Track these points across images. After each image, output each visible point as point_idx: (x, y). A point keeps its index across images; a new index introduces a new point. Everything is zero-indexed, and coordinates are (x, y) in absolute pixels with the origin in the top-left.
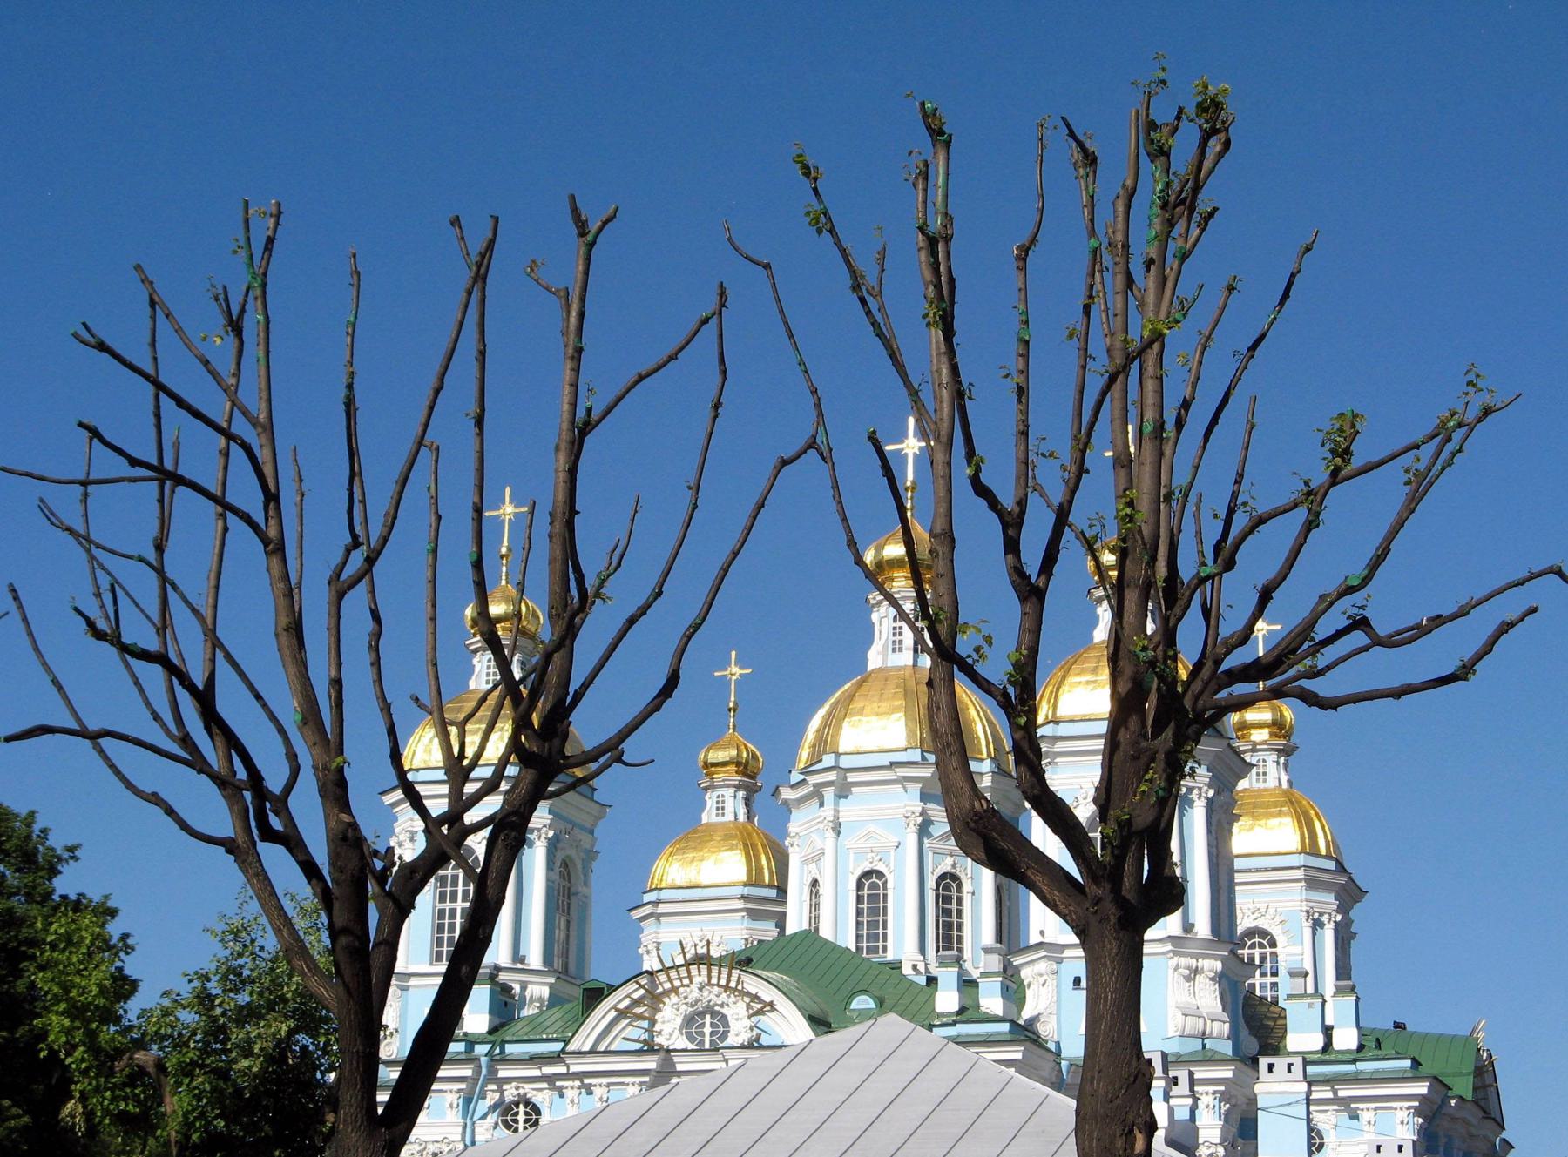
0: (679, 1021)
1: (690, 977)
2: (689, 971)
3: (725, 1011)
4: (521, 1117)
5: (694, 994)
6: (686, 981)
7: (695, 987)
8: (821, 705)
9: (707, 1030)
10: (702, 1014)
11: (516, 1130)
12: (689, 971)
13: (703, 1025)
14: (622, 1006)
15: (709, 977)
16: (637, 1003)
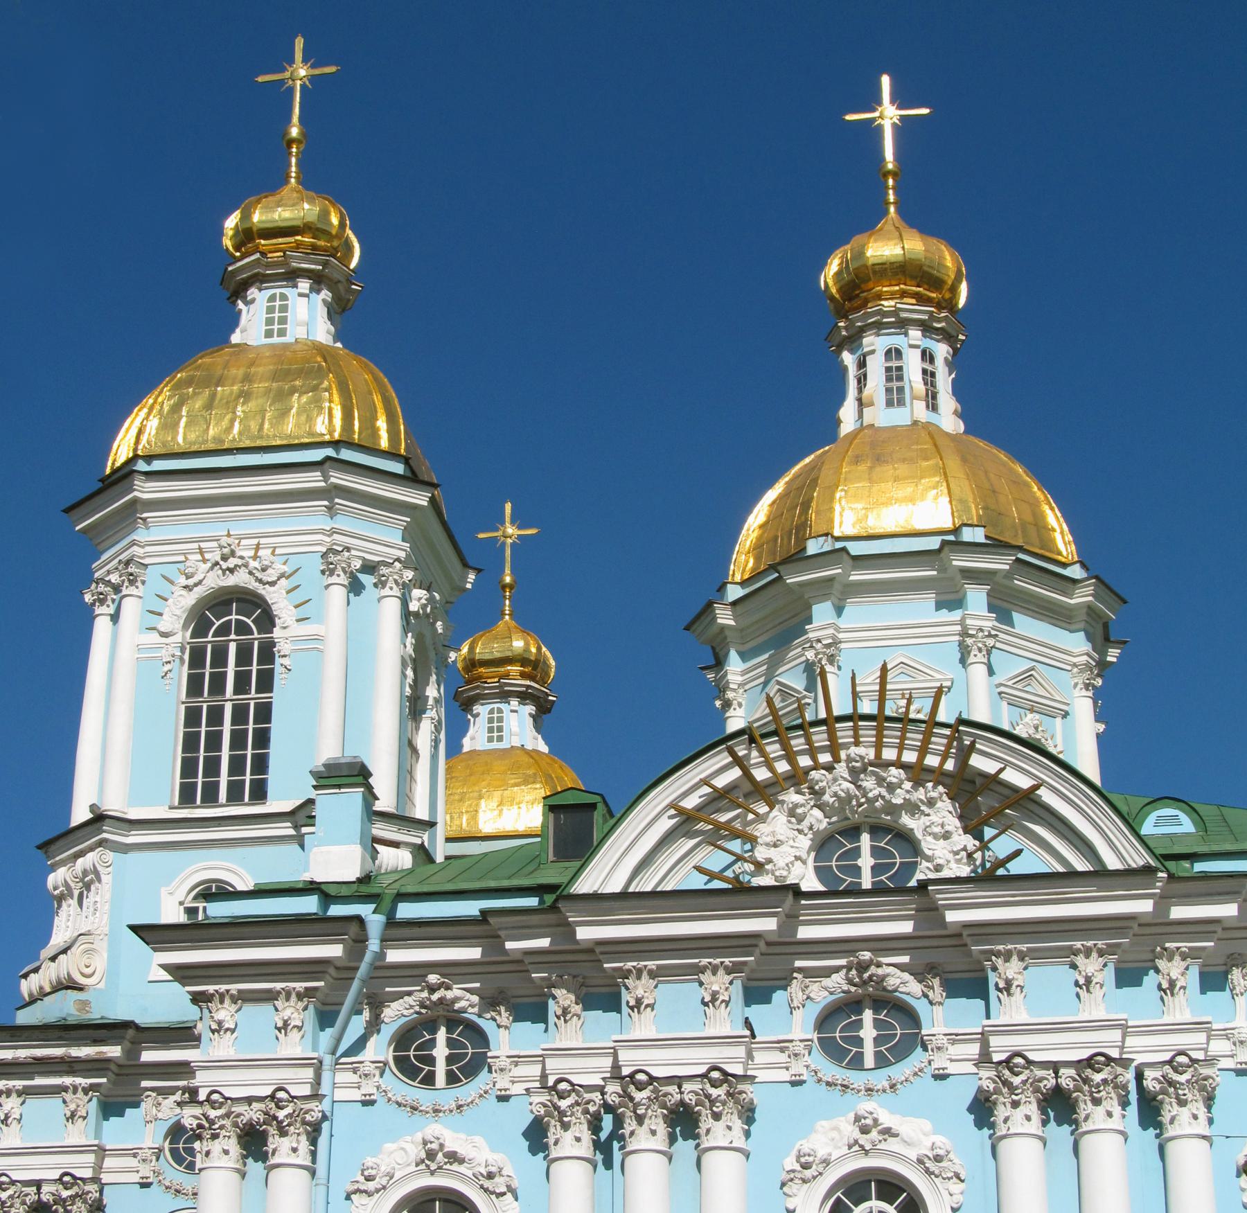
0: (805, 842)
1: (834, 748)
2: (832, 735)
3: (906, 820)
4: (441, 1052)
5: (838, 784)
6: (825, 758)
7: (841, 769)
8: (770, 485)
9: (866, 862)
10: (853, 832)
11: (429, 1080)
12: (832, 735)
13: (856, 853)
14: (690, 803)
15: (879, 746)
16: (721, 798)
